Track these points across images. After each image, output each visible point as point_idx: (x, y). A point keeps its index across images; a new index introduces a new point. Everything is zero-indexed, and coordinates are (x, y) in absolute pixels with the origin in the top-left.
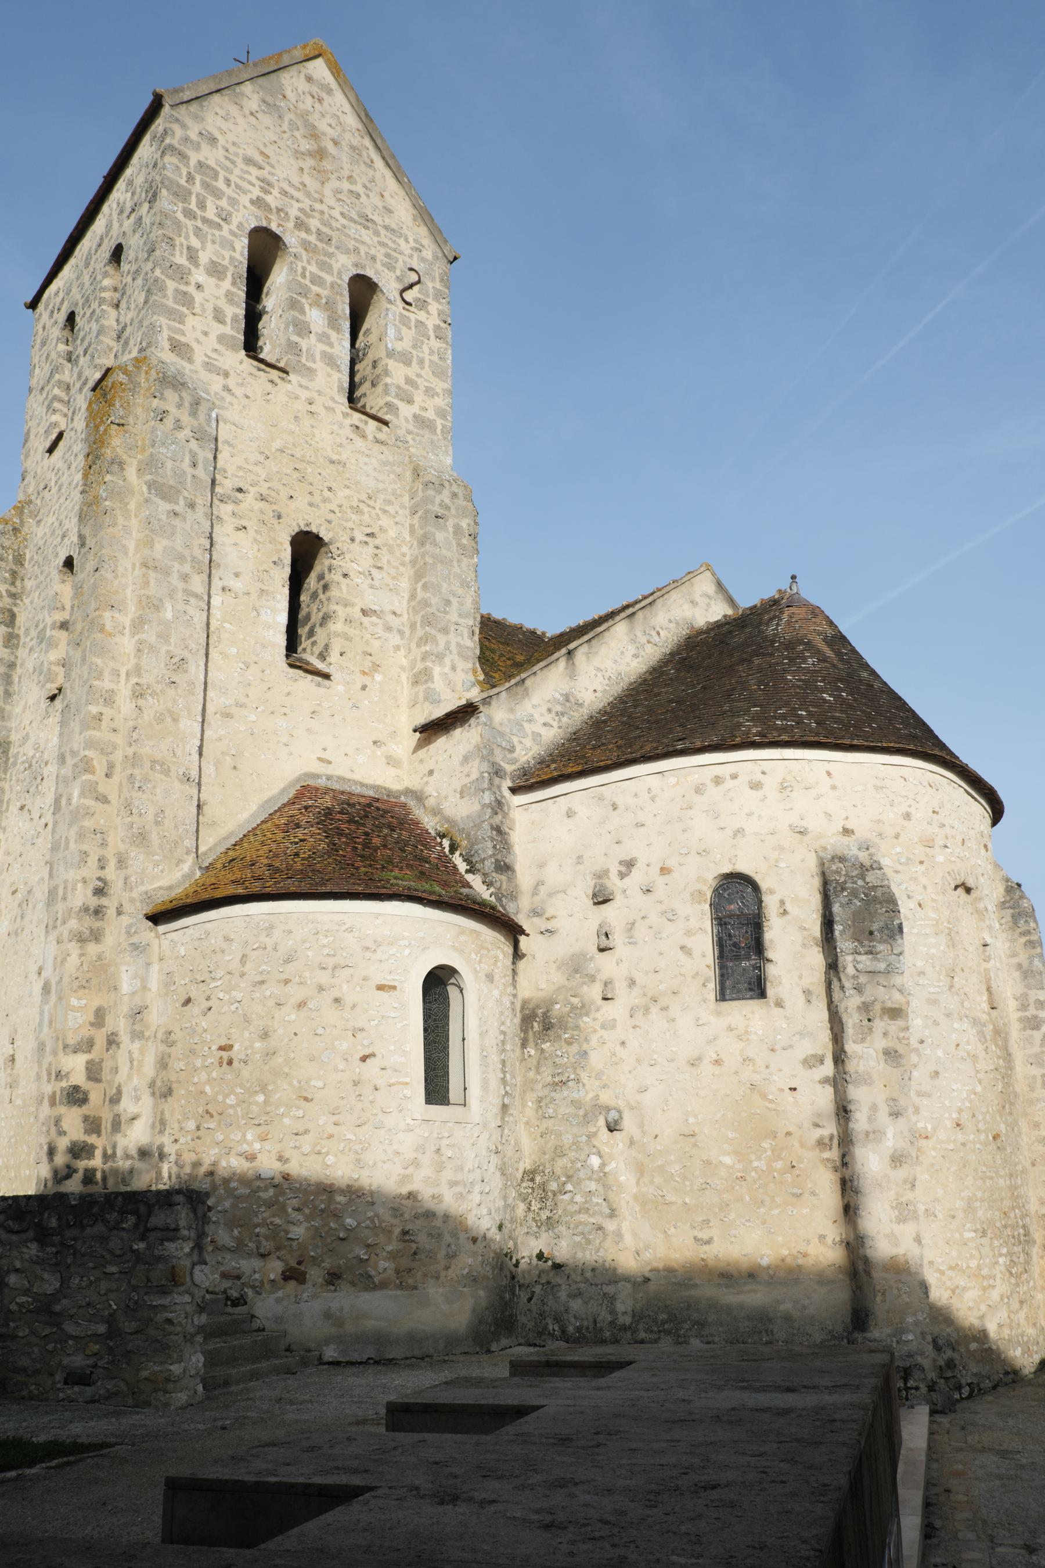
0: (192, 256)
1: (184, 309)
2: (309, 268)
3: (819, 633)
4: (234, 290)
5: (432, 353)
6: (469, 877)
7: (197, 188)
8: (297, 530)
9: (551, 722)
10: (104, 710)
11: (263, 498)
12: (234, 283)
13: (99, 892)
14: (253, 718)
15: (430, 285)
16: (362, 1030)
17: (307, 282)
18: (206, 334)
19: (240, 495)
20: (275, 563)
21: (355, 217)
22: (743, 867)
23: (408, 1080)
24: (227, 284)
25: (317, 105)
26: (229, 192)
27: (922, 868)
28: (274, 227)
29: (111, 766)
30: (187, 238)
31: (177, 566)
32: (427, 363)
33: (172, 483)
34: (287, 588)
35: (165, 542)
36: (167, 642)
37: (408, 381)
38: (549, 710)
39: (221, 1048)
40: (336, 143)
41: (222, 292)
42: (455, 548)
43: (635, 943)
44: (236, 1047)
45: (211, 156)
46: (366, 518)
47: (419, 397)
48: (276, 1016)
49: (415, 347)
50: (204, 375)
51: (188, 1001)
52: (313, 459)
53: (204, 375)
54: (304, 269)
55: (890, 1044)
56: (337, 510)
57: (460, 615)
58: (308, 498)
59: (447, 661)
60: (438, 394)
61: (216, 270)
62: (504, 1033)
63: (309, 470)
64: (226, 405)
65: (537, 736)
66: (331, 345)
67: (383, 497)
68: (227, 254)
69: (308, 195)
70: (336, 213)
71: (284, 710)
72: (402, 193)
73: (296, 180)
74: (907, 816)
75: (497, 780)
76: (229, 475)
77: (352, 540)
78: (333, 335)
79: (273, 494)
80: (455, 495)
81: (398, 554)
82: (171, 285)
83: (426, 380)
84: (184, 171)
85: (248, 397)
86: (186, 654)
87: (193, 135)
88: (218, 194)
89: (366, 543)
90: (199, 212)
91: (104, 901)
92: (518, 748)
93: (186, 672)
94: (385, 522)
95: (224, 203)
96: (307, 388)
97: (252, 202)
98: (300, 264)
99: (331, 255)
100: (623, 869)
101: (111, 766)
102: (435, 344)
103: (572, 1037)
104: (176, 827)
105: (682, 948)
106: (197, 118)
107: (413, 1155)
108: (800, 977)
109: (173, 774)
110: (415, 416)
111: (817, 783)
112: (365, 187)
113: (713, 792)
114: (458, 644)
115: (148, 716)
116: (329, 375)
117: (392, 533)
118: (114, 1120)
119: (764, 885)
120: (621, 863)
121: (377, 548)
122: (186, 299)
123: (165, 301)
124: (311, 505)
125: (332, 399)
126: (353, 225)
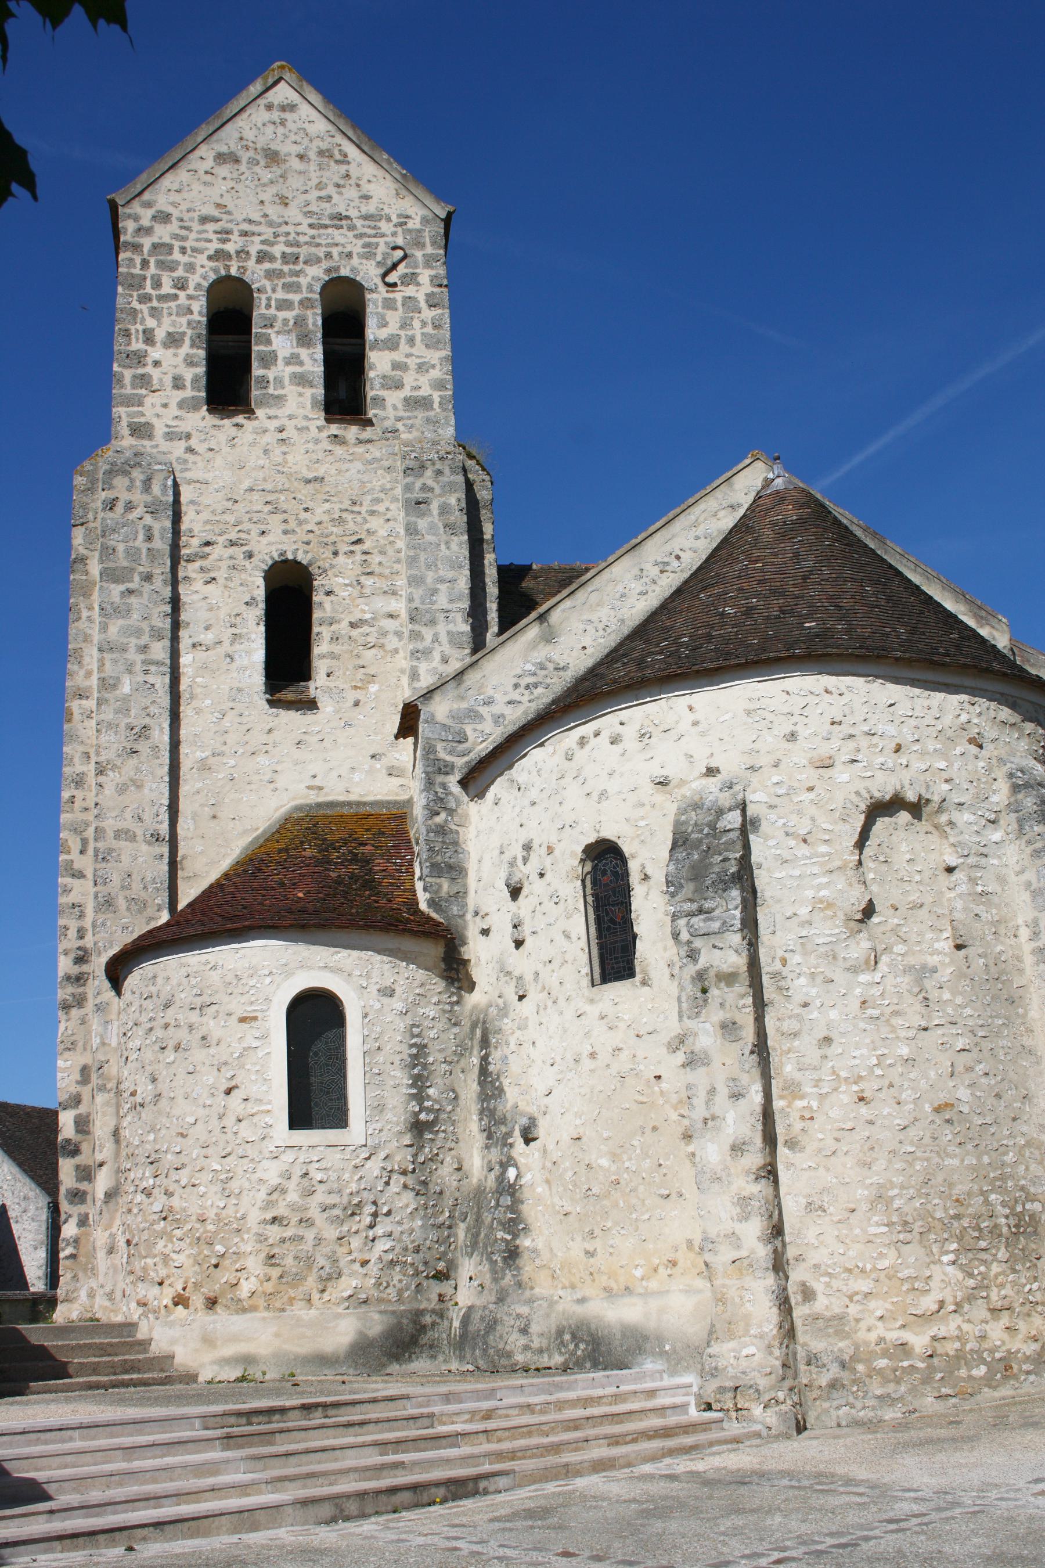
0: (149, 337)
1: (143, 392)
2: (274, 296)
4: (195, 351)
5: (424, 324)
7: (153, 269)
8: (270, 562)
9: (518, 698)
10: (76, 793)
11: (232, 543)
12: (193, 345)
13: (80, 960)
14: (232, 762)
15: (419, 254)
16: (226, 1063)
17: (273, 311)
18: (165, 406)
19: (207, 549)
20: (247, 603)
21: (327, 222)
23: (269, 1107)
24: (186, 349)
25: (281, 130)
26: (184, 259)
27: (811, 795)
28: (233, 272)
29: (85, 842)
30: (143, 320)
31: (133, 641)
32: (418, 338)
33: (125, 564)
34: (262, 624)
35: (121, 622)
36: (129, 716)
37: (396, 366)
40: (301, 157)
41: (180, 358)
42: (442, 530)
45: (163, 233)
46: (351, 526)
47: (409, 379)
49: (403, 327)
50: (165, 446)
52: (286, 486)
53: (165, 446)
54: (269, 299)
55: (728, 1016)
56: (315, 528)
57: (451, 601)
58: (284, 527)
59: (437, 656)
60: (433, 366)
61: (173, 340)
63: (283, 498)
64: (190, 465)
65: (498, 719)
66: (301, 364)
67: (369, 497)
68: (184, 320)
69: (271, 224)
70: (304, 228)
71: (266, 748)
72: (381, 173)
73: (256, 216)
74: (792, 737)
75: (440, 779)
76: (196, 532)
78: (304, 353)
79: (243, 536)
80: (439, 473)
81: (390, 552)
82: (128, 374)
83: (418, 357)
84: (138, 261)
85: (211, 450)
86: (147, 721)
87: (146, 222)
88: (171, 267)
89: (352, 552)
90: (153, 293)
91: (85, 968)
93: (148, 738)
94: (374, 523)
95: (180, 272)
96: (276, 417)
97: (210, 258)
98: (263, 297)
99: (297, 274)
101: (85, 842)
102: (428, 314)
104: (145, 888)
106: (148, 205)
107: (278, 1180)
108: (665, 949)
109: (140, 838)
110: (406, 400)
111: (677, 723)
112: (338, 186)
113: (580, 755)
114: (448, 633)
115: (109, 790)
116: (300, 395)
117: (382, 533)
119: (626, 850)
121: (366, 553)
122: (143, 380)
123: (123, 391)
124: (285, 532)
125: (306, 418)
126: (322, 231)
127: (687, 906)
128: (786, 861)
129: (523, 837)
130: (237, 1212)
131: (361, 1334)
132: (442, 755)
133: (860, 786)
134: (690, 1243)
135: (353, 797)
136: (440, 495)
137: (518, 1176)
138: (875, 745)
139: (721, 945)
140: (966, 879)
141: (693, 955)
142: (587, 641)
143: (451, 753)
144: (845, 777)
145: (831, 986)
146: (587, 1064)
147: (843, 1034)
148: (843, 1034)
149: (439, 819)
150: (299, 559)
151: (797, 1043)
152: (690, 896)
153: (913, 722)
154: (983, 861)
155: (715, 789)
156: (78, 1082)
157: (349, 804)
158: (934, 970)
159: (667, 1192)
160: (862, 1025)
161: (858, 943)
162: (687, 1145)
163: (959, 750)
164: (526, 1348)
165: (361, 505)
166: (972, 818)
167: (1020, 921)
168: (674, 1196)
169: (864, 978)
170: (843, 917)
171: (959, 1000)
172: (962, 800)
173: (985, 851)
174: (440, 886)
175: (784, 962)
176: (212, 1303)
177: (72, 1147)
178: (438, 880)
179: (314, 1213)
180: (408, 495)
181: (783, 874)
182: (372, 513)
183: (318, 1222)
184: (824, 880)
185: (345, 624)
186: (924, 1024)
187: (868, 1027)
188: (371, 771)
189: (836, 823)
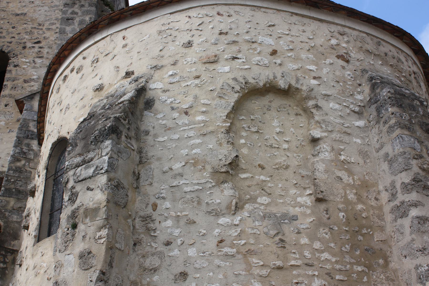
27: (197, 81)
55: (86, 247)
67: (49, 22)
74: (189, 44)
75: (26, 141)
77: (24, 48)
89: (33, 47)
128: (169, 129)
133: (239, 75)
136: (81, 16)
138: (255, 49)
140: (329, 149)
144: (227, 69)
145: (192, 228)
147: (197, 270)
148: (197, 270)
149: (18, 164)
150: (4, 50)
151: (156, 278)
153: (289, 38)
154: (346, 138)
158: (294, 218)
160: (217, 262)
161: (222, 191)
163: (328, 61)
165: (44, 26)
166: (337, 106)
167: (381, 188)
169: (222, 220)
170: (210, 170)
171: (317, 245)
172: (329, 93)
173: (349, 131)
174: (8, 202)
175: (155, 207)
178: (8, 199)
180: (64, 16)
181: (166, 138)
182: (49, 29)
184: (198, 141)
185: (21, 80)
186: (279, 263)
187: (222, 264)
189: (214, 99)
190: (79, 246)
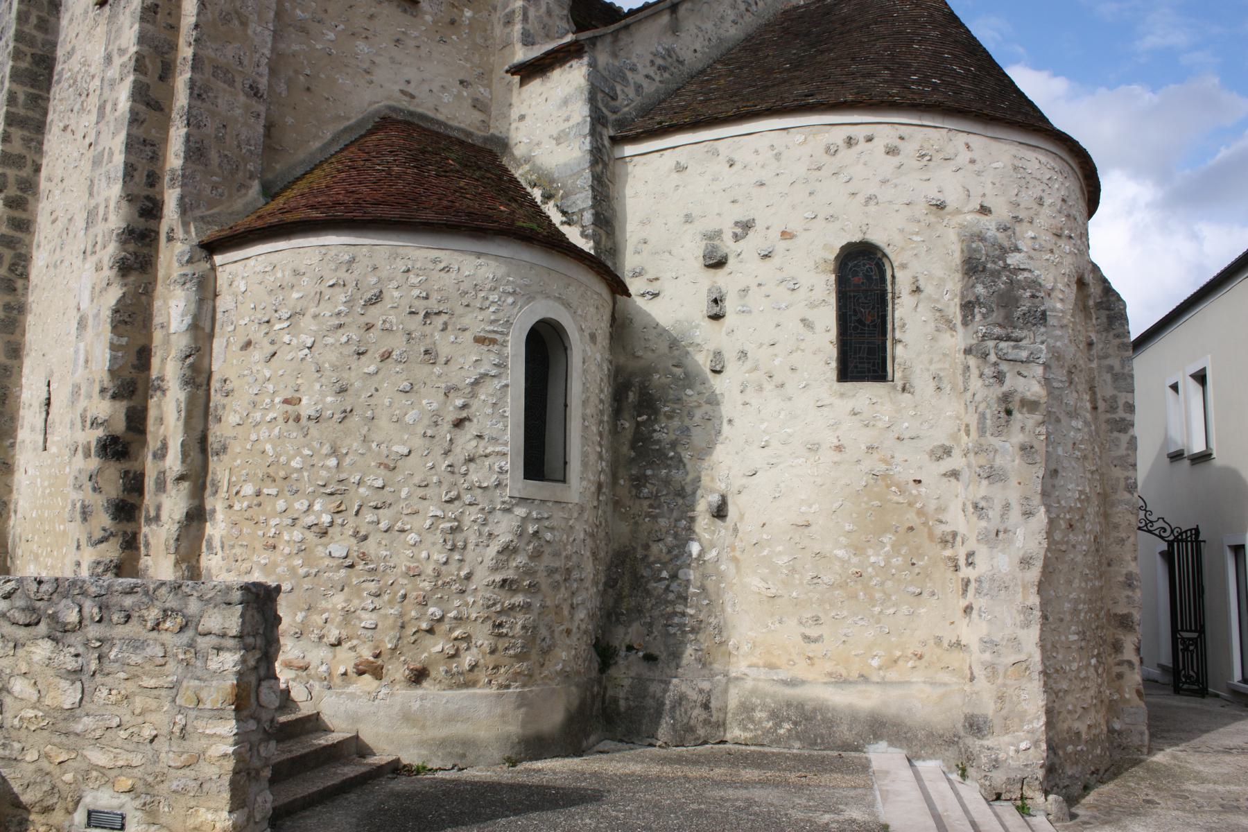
3: (936, 9)
6: (565, 229)
9: (652, 74)
14: (331, 36)
22: (876, 237)
38: (652, 62)
39: (286, 401)
43: (750, 312)
44: (304, 401)
48: (353, 367)
51: (248, 344)
62: (601, 401)
65: (639, 88)
92: (621, 96)
100: (738, 231)
103: (673, 411)
104: (239, 146)
105: (803, 320)
108: (931, 362)
109: (238, 85)
113: (847, 155)
118: (158, 478)
120: (736, 223)
127: (997, 331)
129: (740, 213)
130: (460, 569)
131: (567, 710)
132: (600, 105)
134: (938, 641)
135: (441, 117)
137: (702, 552)
139: (1025, 373)
141: (1000, 377)
142: (698, 46)
143: (606, 106)
146: (828, 456)
152: (1000, 320)
155: (993, 226)
156: (134, 367)
157: (432, 120)
159: (918, 591)
162: (944, 548)
164: (707, 722)
168: (925, 595)
176: (419, 676)
177: (120, 448)
179: (541, 578)
183: (543, 587)
188: (458, 97)
190: (1018, 438)
